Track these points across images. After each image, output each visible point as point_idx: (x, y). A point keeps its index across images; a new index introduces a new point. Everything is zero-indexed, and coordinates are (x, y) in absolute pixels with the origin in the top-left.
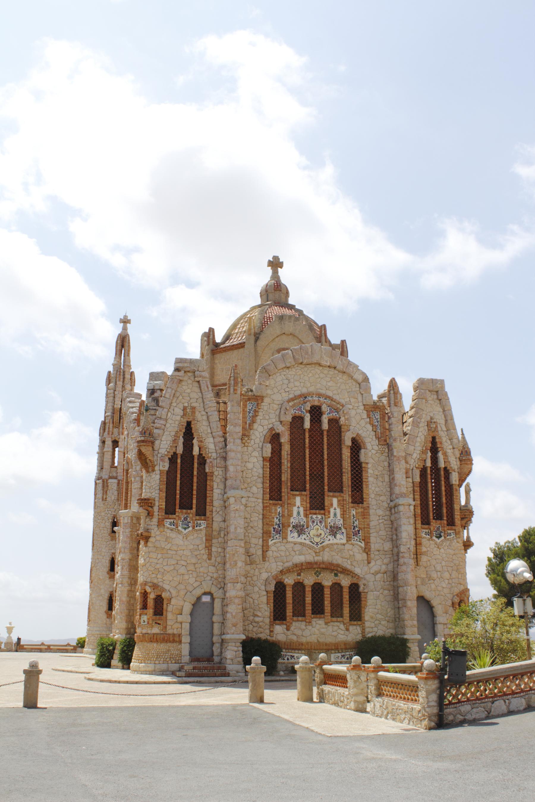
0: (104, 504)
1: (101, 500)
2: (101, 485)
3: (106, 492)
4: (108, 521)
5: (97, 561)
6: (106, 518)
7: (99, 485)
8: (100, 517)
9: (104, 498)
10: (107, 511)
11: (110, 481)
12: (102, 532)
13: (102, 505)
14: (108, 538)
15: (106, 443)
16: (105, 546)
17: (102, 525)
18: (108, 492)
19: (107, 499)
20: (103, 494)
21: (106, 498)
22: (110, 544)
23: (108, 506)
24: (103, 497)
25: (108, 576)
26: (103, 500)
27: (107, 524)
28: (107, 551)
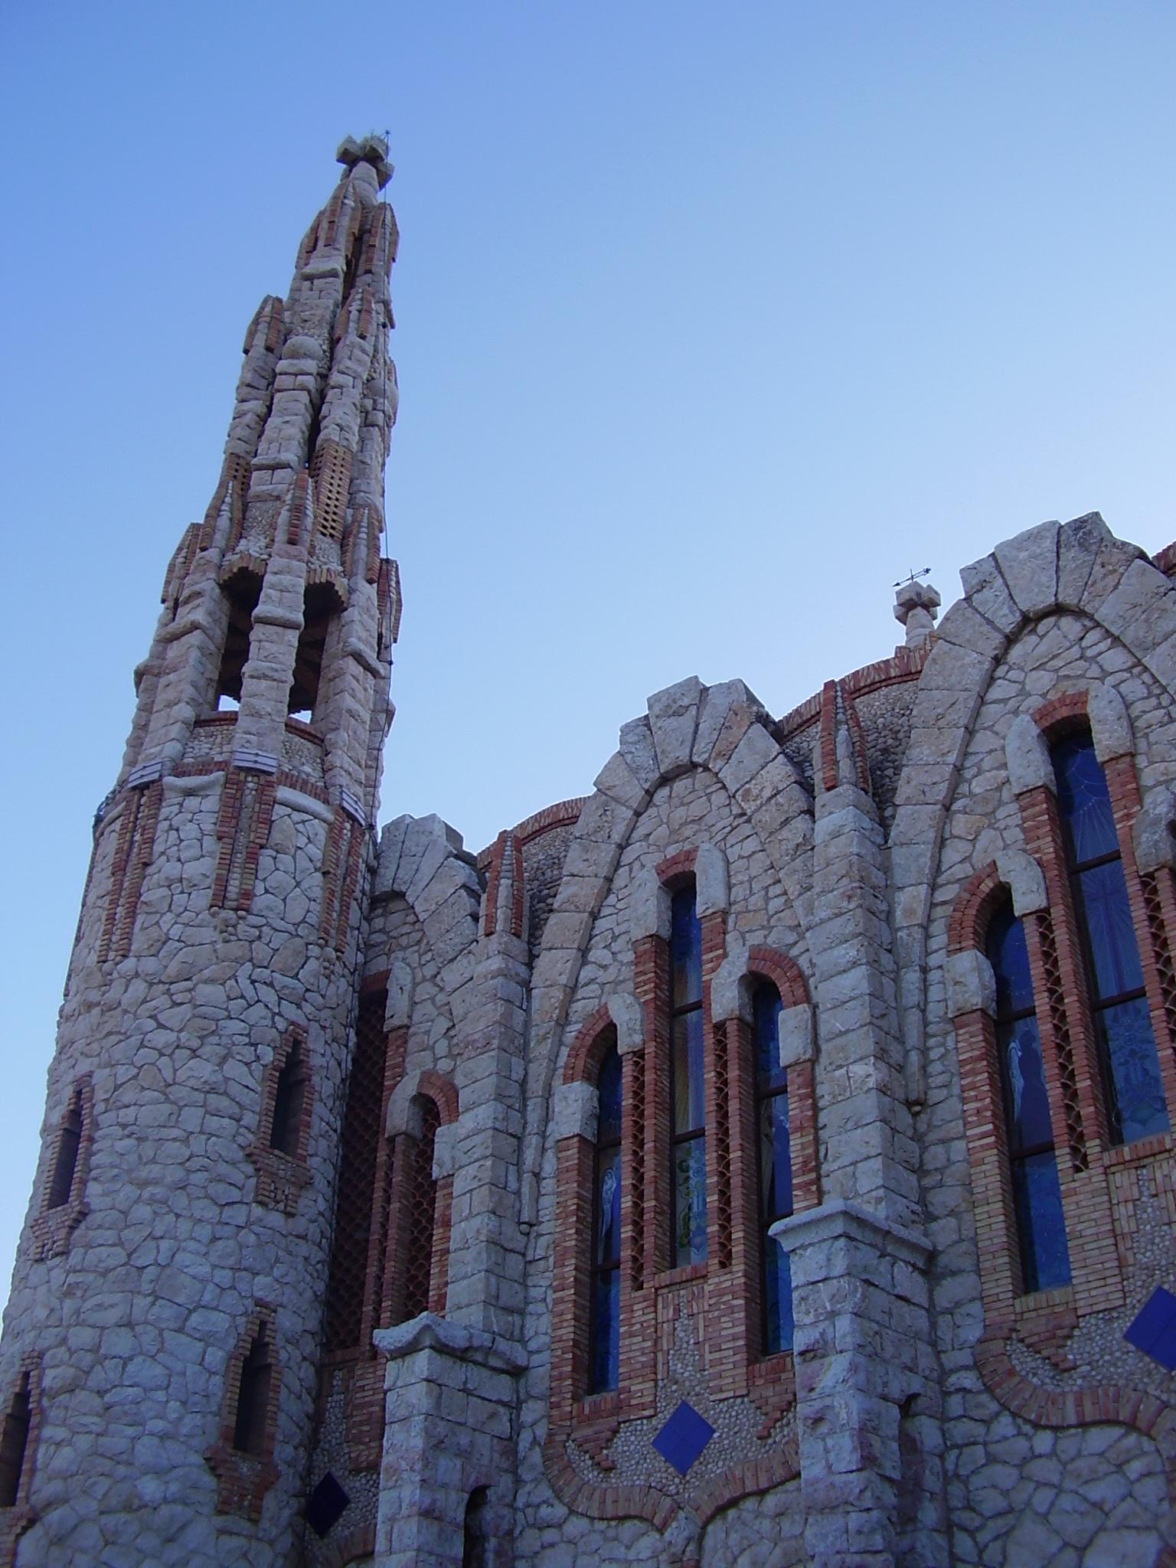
0: (227, 930)
1: (202, 899)
2: (212, 803)
3: (253, 857)
4: (248, 1053)
5: (121, 1343)
6: (235, 1026)
7: (192, 803)
8: (186, 1010)
9: (233, 890)
10: (244, 983)
11: (284, 793)
12: (192, 1118)
13: (208, 934)
14: (238, 1177)
15: (269, 579)
16: (204, 1232)
17: (203, 1070)
18: (265, 859)
19: (260, 902)
20: (227, 863)
21: (248, 895)
22: (248, 1224)
23: (261, 951)
24: (222, 883)
25: (209, 1481)
26: (220, 900)
27: (233, 1068)
28: (224, 1277)
